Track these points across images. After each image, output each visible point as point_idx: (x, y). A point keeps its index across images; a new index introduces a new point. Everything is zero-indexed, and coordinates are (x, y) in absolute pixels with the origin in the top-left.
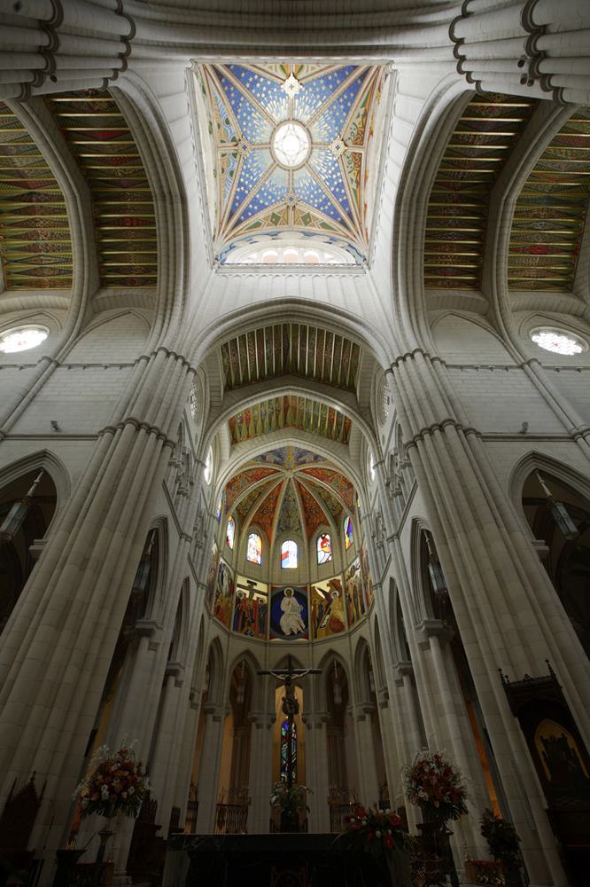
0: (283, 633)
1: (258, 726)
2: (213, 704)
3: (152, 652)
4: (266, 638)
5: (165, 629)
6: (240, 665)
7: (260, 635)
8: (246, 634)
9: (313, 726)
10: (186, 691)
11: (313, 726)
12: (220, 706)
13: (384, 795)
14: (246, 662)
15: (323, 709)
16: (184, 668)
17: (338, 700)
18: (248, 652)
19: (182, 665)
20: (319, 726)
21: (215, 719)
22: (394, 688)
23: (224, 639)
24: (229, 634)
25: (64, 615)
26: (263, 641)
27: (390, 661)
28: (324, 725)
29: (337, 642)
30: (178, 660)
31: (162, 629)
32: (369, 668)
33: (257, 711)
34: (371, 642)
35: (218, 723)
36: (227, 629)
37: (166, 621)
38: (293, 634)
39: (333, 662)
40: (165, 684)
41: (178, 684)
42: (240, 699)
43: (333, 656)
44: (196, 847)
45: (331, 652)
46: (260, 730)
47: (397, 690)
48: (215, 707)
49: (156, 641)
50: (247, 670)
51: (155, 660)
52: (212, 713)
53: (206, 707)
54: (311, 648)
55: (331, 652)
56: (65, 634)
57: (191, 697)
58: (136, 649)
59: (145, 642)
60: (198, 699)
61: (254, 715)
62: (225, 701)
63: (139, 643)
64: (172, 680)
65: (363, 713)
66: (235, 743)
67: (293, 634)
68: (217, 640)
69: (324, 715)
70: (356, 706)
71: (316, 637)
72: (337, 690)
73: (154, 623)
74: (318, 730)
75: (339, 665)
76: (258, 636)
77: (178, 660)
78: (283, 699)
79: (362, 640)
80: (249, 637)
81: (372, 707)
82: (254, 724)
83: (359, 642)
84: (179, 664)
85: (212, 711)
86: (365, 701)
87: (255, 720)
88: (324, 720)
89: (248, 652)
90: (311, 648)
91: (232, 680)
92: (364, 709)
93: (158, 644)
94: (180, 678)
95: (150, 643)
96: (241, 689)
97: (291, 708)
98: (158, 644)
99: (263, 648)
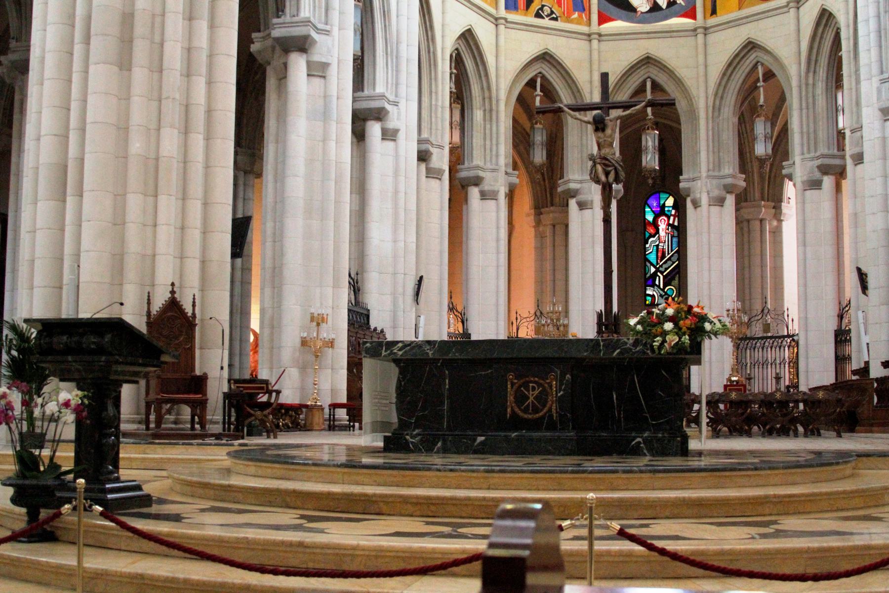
0: (632, 9)
1: (582, 206)
2: (478, 167)
3: (317, 81)
4: (589, 24)
5: (335, 31)
6: (531, 84)
7: (576, 15)
8: (538, 15)
9: (704, 201)
10: (409, 147)
11: (704, 201)
12: (494, 170)
13: (845, 321)
14: (543, 77)
15: (730, 168)
16: (396, 104)
17: (761, 149)
18: (546, 57)
19: (392, 98)
20: (720, 202)
21: (484, 196)
22: (877, 124)
23: (485, 33)
24: (496, 21)
25: (126, 41)
26: (584, 29)
27: (875, 69)
28: (730, 200)
29: (763, 24)
30: (380, 89)
31: (327, 33)
32: (836, 80)
33: (580, 178)
34: (843, 19)
35: (492, 203)
36: (492, 10)
37: (335, 16)
38: (655, 8)
39: (755, 67)
40: (359, 135)
41: (389, 135)
42: (539, 156)
43: (753, 57)
44: (401, 353)
45: (751, 46)
46: (587, 213)
47: (883, 129)
48: (481, 174)
49: (324, 60)
50: (549, 93)
51: (326, 97)
52: (476, 185)
53: (463, 174)
54: (700, 37)
55: (751, 46)
56: (140, 75)
57: (423, 157)
58: (283, 76)
59: (298, 64)
60: (441, 160)
61: (573, 186)
62: (502, 161)
63: (285, 65)
64: (374, 129)
65: (817, 175)
66: (540, 236)
67: (655, 8)
68: (468, 37)
69: (729, 181)
70: (803, 160)
71: (714, 12)
72: (760, 128)
73: (307, 22)
74: (715, 210)
75: (769, 75)
76: (568, 20)
77: (380, 89)
78: (592, 158)
79: (825, 17)
80: (546, 22)
81: (837, 162)
82: (573, 203)
83: (818, 24)
84: (382, 96)
85: (477, 181)
86: (823, 150)
87: (573, 194)
88: (729, 189)
89: (546, 57)
90: (700, 37)
91: (515, 120)
92: (819, 167)
93: (325, 66)
94: (391, 124)
95: (309, 64)
96: (539, 137)
97: (607, 174)
98: (325, 66)
99: (584, 44)
